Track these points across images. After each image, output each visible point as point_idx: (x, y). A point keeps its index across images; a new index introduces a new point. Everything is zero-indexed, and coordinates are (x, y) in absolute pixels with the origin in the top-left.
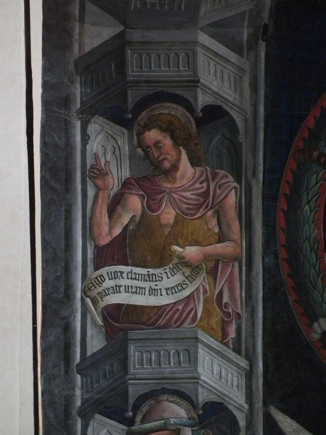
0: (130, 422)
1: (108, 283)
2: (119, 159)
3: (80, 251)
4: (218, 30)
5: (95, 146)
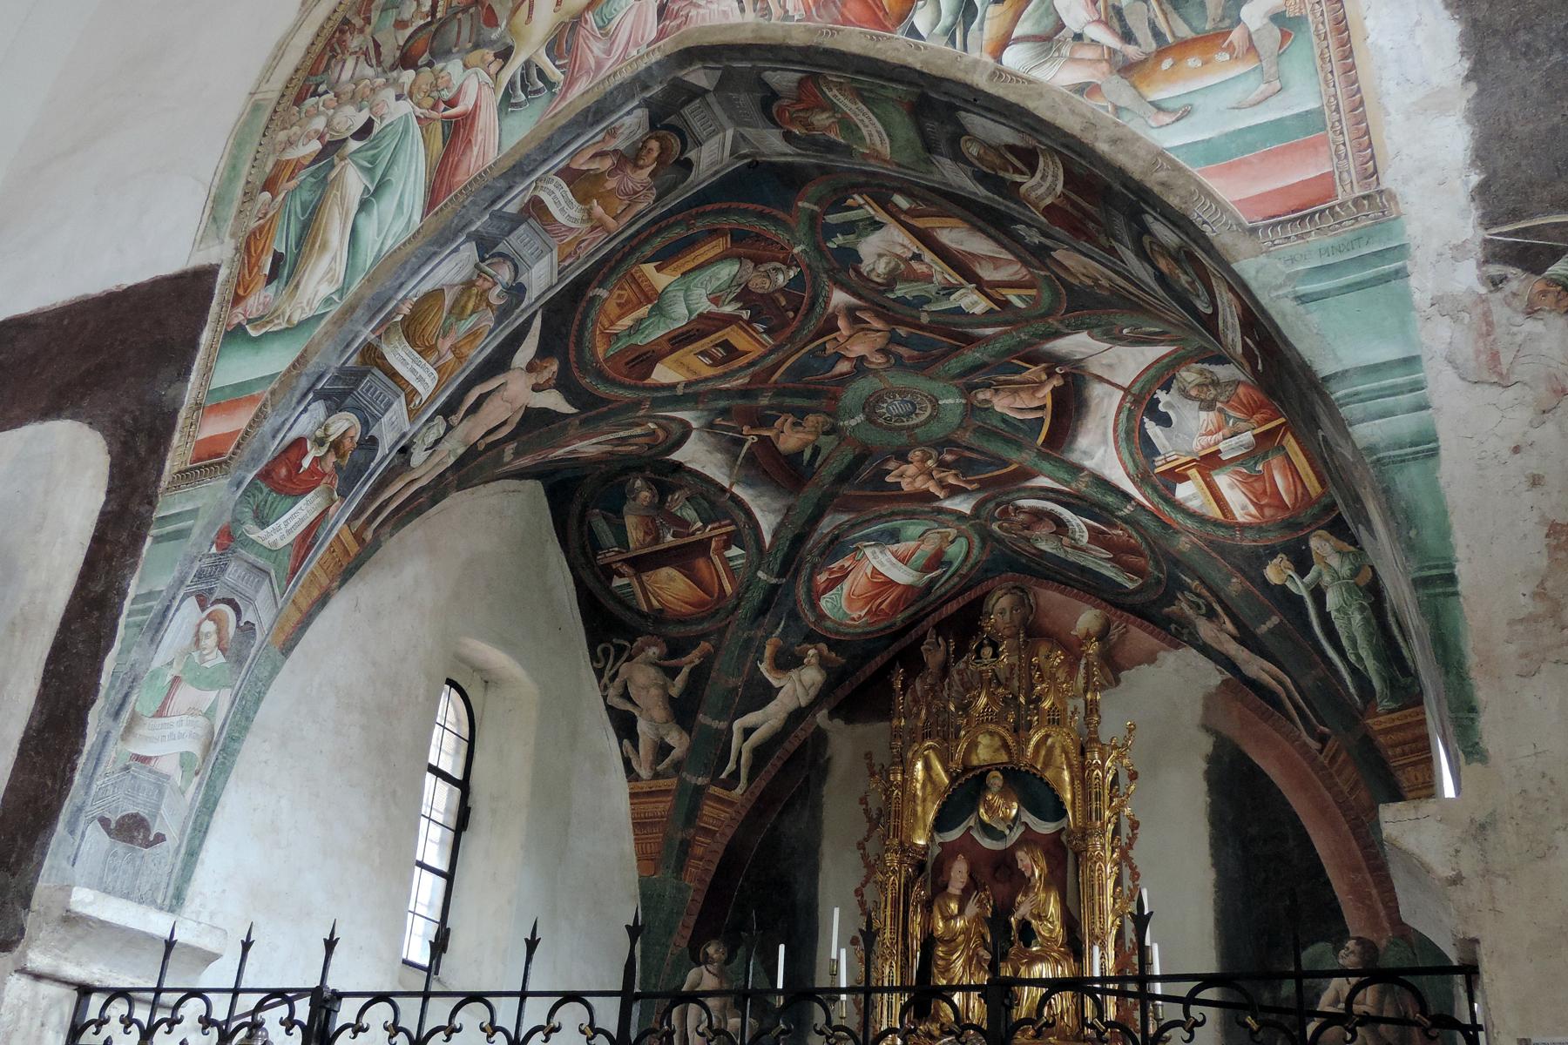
0: (483, 260)
1: (551, 186)
2: (627, 138)
3: (560, 160)
4: (739, 139)
5: (628, 120)
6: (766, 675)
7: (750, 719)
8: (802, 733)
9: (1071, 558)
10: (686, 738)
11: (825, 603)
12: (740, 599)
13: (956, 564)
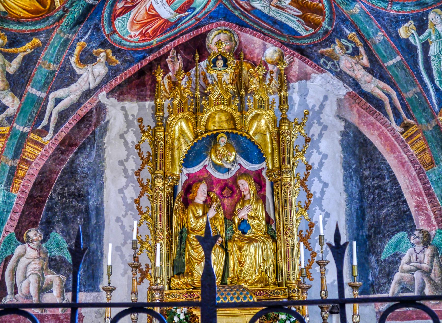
6: (73, 65)
7: (60, 93)
8: (89, 105)
9: (271, 14)
10: (17, 100)
11: (118, 23)
12: (65, 11)
13: (198, 10)
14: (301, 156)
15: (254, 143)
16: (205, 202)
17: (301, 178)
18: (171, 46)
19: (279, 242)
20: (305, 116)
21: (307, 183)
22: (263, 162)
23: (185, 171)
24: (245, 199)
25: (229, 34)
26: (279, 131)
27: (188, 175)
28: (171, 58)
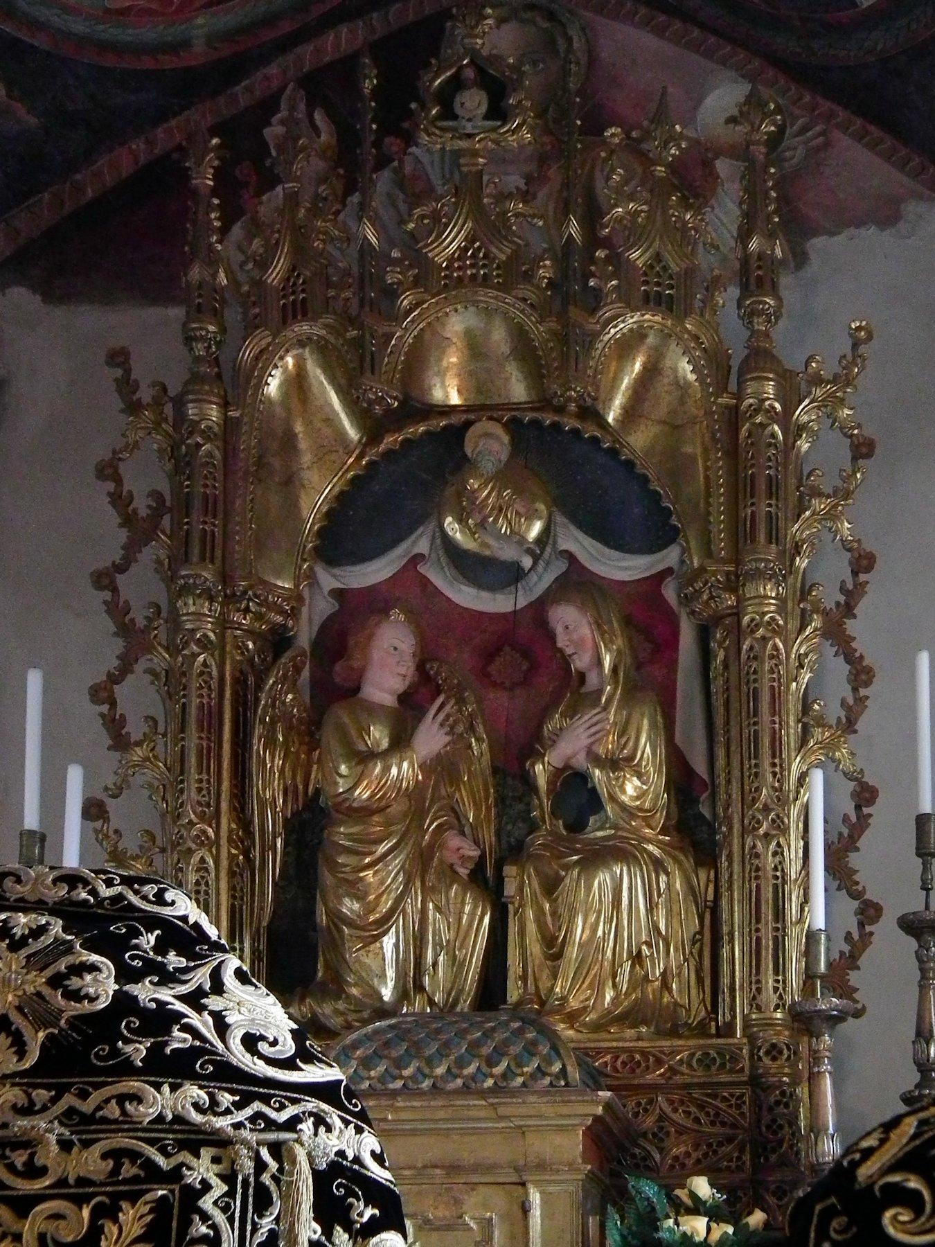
14: (832, 515)
15: (629, 464)
16: (404, 698)
17: (829, 604)
18: (284, 72)
19: (725, 864)
20: (855, 346)
21: (851, 626)
22: (665, 546)
23: (328, 580)
24: (583, 690)
25: (546, 25)
26: (737, 407)
27: (339, 594)
28: (282, 122)
